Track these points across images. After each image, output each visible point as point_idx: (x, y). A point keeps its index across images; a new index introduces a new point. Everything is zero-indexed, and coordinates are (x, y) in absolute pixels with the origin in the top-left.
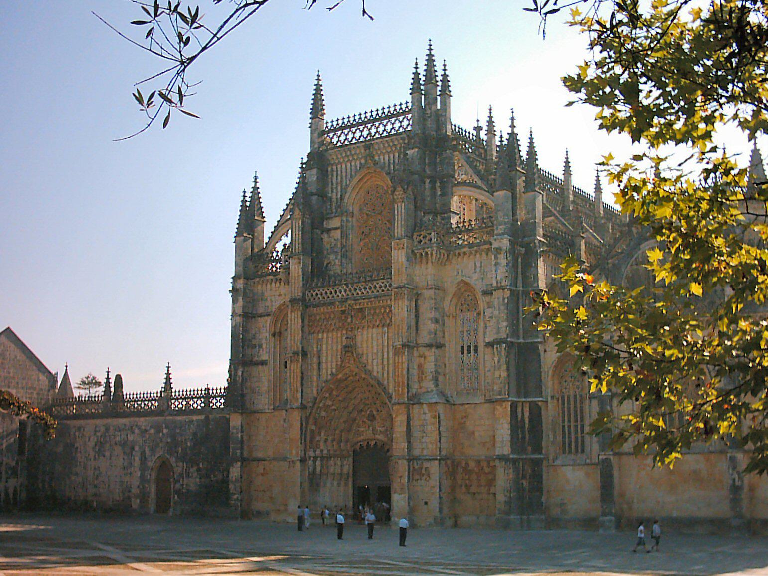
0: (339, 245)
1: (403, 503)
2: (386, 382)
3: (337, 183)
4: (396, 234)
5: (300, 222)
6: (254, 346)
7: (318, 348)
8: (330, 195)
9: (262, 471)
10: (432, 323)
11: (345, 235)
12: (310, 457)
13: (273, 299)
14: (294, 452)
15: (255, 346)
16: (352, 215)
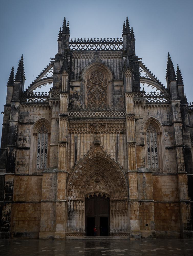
0: (79, 94)
1: (137, 225)
2: (119, 161)
3: (77, 66)
4: (127, 90)
5: (67, 77)
6: (20, 139)
7: (74, 141)
8: (73, 71)
9: (22, 209)
10: (143, 134)
11: (82, 90)
12: (68, 200)
13: (34, 116)
14: (61, 197)
15: (20, 139)
16: (85, 82)
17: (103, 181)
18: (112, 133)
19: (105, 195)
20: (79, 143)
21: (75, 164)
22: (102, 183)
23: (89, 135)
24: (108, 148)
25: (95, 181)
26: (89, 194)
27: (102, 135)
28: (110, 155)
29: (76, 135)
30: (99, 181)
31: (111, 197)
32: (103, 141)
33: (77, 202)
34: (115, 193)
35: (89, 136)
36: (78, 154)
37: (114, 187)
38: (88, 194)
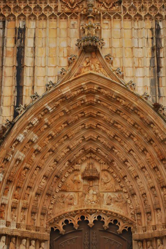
17: (109, 175)
18: (141, 19)
19: (116, 221)
20: (30, 49)
21: (16, 114)
22: (105, 183)
23: (63, 24)
24: (128, 62)
25: (83, 174)
26: (64, 219)
27: (107, 24)
28: (133, 85)
29: (20, 24)
30: (95, 175)
31: (135, 228)
32: (110, 42)
33: (21, 243)
34: (150, 213)
35: (66, 27)
36: (27, 82)
37: (148, 193)
38: (60, 218)
